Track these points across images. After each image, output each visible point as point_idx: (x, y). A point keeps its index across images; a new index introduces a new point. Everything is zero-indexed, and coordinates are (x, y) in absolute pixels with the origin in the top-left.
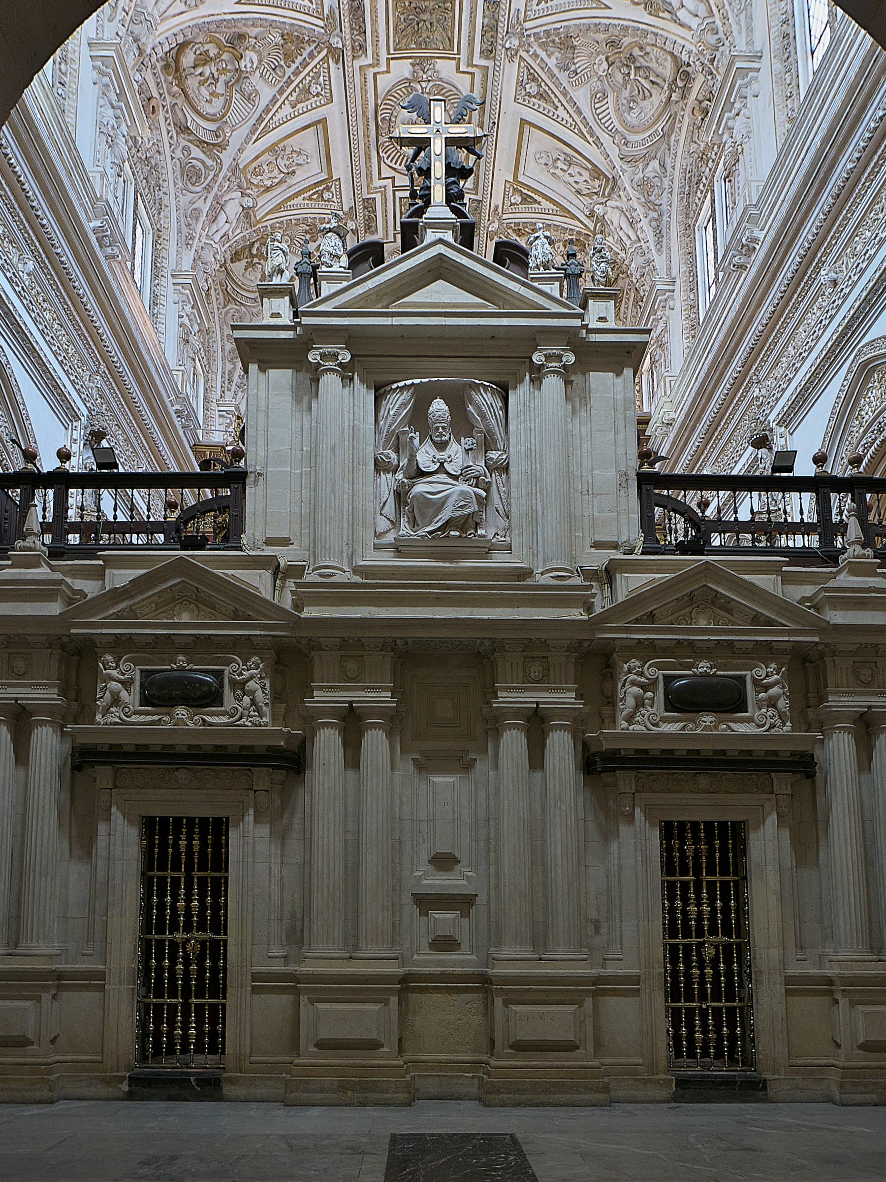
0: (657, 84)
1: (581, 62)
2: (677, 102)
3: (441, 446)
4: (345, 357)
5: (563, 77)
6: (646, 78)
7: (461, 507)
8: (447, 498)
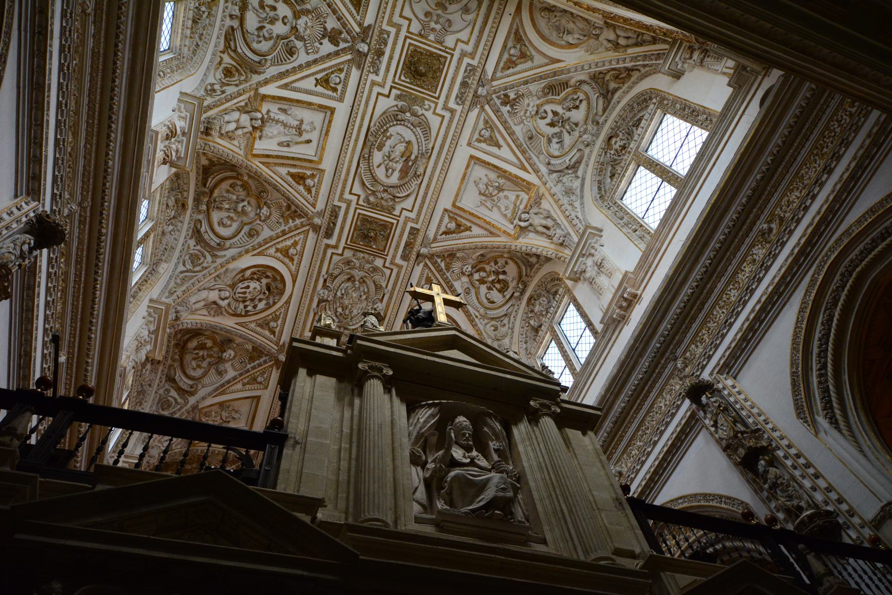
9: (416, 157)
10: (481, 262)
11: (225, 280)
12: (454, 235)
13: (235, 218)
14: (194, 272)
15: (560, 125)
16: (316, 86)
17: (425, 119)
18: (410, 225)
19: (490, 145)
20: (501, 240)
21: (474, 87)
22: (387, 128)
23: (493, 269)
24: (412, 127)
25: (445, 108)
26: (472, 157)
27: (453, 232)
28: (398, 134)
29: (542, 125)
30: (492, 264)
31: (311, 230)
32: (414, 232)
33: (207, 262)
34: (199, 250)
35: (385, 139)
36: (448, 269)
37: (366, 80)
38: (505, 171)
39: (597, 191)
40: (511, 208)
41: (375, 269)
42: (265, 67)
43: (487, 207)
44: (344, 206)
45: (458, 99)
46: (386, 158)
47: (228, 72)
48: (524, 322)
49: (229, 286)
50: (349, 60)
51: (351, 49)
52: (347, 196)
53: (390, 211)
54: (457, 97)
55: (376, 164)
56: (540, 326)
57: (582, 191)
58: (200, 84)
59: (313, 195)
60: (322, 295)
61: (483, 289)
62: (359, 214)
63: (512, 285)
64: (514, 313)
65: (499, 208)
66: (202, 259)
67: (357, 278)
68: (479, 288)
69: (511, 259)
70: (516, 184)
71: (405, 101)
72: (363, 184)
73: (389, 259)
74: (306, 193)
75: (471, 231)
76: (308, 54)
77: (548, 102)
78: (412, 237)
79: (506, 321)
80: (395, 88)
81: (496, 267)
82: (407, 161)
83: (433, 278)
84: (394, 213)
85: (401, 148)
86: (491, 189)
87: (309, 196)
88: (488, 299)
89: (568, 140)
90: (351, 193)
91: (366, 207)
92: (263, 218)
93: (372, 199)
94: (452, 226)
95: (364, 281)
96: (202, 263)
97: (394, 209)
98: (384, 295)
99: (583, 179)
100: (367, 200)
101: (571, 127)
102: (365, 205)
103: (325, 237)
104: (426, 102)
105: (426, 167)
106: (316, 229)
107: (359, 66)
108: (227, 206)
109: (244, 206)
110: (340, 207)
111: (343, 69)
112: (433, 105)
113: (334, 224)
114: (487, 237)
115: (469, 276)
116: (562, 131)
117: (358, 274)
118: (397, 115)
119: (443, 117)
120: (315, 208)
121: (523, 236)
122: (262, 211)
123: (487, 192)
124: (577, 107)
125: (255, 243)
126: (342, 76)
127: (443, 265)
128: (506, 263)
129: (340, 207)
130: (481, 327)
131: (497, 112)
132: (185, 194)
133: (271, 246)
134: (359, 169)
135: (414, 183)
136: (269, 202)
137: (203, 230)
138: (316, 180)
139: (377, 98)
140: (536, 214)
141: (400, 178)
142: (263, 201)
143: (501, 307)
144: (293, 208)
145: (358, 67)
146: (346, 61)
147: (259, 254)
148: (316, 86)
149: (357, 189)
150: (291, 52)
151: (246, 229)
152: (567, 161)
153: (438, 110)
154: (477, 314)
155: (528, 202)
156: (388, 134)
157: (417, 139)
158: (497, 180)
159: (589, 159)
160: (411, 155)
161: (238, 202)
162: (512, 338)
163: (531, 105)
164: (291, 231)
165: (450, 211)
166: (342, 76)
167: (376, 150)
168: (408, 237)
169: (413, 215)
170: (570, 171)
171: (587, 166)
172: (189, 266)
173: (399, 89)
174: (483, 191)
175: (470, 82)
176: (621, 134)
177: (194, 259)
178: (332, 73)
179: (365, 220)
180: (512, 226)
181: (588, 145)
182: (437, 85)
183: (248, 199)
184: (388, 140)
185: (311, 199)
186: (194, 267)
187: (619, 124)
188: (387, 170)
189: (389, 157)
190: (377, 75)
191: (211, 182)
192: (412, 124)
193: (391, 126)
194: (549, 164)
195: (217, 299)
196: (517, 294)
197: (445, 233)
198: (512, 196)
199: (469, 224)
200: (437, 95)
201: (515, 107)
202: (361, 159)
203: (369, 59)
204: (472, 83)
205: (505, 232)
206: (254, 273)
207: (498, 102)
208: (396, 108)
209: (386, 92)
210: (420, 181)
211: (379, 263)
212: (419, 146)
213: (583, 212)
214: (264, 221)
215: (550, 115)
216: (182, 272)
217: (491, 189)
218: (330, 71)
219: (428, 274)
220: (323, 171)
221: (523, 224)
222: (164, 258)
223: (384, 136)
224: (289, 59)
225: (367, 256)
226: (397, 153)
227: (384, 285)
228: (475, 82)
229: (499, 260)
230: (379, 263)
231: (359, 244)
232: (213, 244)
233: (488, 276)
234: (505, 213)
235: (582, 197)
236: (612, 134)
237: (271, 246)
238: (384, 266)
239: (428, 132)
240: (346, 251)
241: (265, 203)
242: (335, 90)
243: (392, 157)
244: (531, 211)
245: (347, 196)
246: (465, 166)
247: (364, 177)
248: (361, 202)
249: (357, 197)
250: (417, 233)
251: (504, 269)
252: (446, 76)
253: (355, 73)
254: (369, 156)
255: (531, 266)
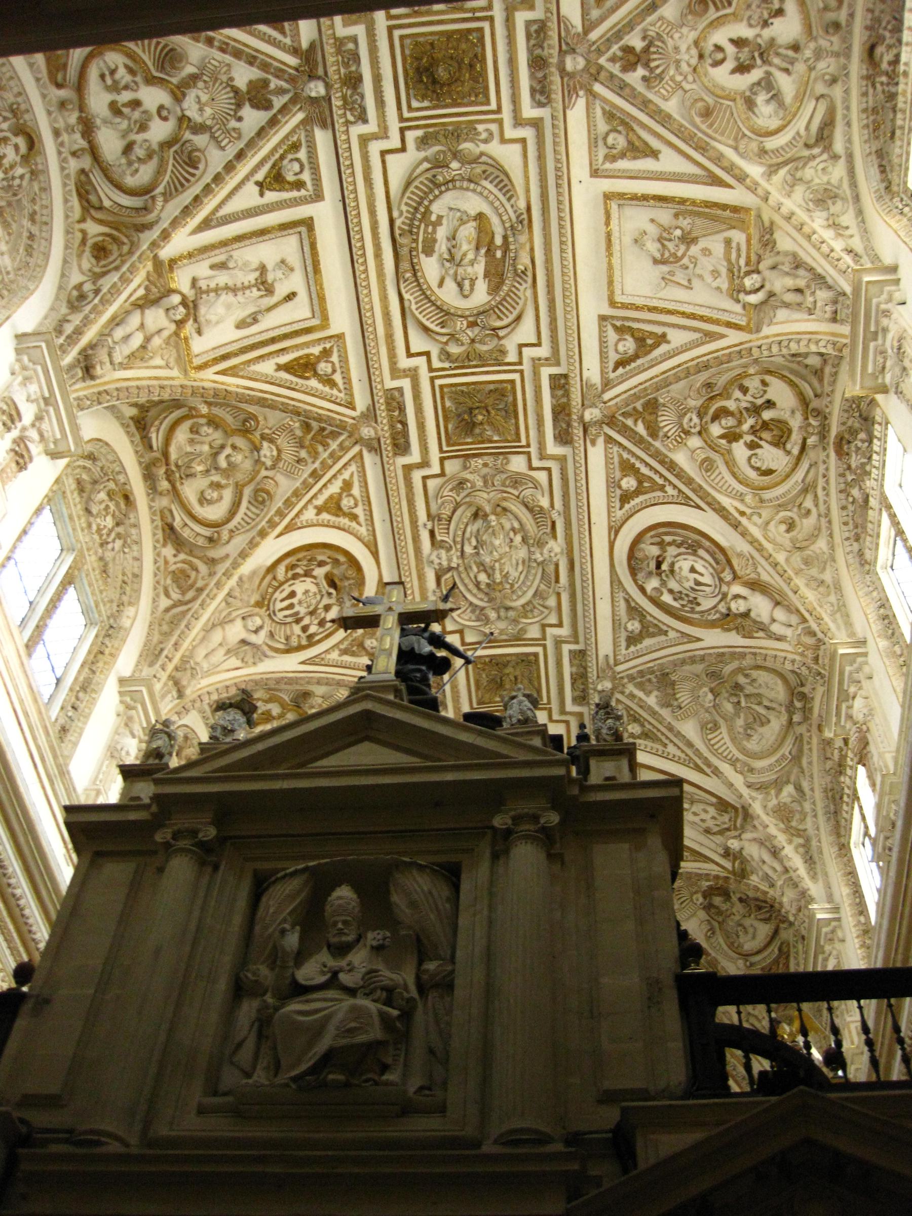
0: (773, 709)
1: (684, 697)
2: (799, 724)
3: (341, 950)
4: (211, 832)
5: (665, 713)
6: (759, 704)
7: (350, 1031)
8: (328, 1018)
9: (505, 238)
10: (711, 398)
11: (245, 597)
12: (639, 362)
13: (224, 482)
14: (187, 603)
15: (759, 62)
16: (262, 195)
17: (490, 161)
18: (546, 372)
19: (635, 158)
20: (734, 337)
21: (554, 60)
22: (427, 208)
23: (744, 405)
24: (472, 186)
25: (518, 122)
26: (608, 197)
27: (636, 357)
28: (451, 209)
29: (722, 76)
30: (737, 394)
31: (365, 453)
32: (560, 383)
33: (203, 578)
34: (184, 562)
35: (430, 229)
36: (654, 433)
37: (348, 141)
38: (683, 201)
39: (878, 176)
40: (724, 271)
41: (517, 480)
42: (156, 213)
43: (679, 284)
44: (405, 384)
45: (538, 96)
46: (447, 265)
47: (100, 251)
48: (843, 496)
49: (259, 604)
50: (303, 122)
51: (294, 100)
52: (404, 362)
53: (497, 357)
54: (533, 91)
55: (433, 281)
56: (866, 500)
57: (854, 184)
58: (57, 298)
59: (341, 386)
60: (437, 561)
61: (740, 451)
62: (441, 387)
63: (796, 422)
64: (821, 482)
65: (701, 277)
66: (193, 574)
67: (488, 509)
68: (729, 452)
69: (769, 372)
70: (714, 219)
71: (439, 142)
72: (426, 329)
73: (533, 450)
74: (327, 389)
75: (668, 342)
76: (223, 149)
77: (715, 24)
78: (560, 393)
79: (808, 503)
80: (409, 128)
81: (749, 397)
82: (490, 253)
83: (633, 460)
84: (508, 360)
85: (468, 231)
86: (670, 245)
87: (335, 392)
88: (757, 469)
89: (786, 84)
90: (410, 355)
91: (451, 368)
92: (269, 463)
93: (454, 349)
94: (629, 345)
95: (505, 509)
96: (195, 582)
97: (503, 352)
98: (554, 523)
99: (850, 157)
100: (446, 355)
101: (784, 58)
102: (447, 365)
103: (395, 454)
104: (480, 128)
105: (532, 249)
106: (374, 446)
107: (327, 123)
108: (200, 468)
109: (228, 456)
110: (400, 390)
111: (299, 140)
112: (494, 127)
113: (404, 424)
114: (703, 344)
115: (700, 433)
116: (768, 74)
117: (484, 499)
118: (434, 176)
119: (523, 141)
120: (354, 409)
121: (766, 321)
122: (262, 453)
123: (667, 255)
124: (780, 12)
125: (272, 512)
126: (302, 154)
127: (641, 429)
128: (764, 383)
129: (400, 390)
130: (756, 532)
131: (621, 88)
132: (121, 478)
133: (305, 507)
134: (406, 304)
135: (522, 288)
136: (267, 431)
137: (177, 524)
138: (335, 358)
139: (384, 162)
140: (774, 268)
141: (494, 289)
142: (257, 434)
143: (788, 476)
144: (315, 425)
145: (324, 126)
146: (297, 126)
147: (289, 529)
148: (262, 195)
149: (418, 343)
150: (191, 161)
151: (247, 492)
152: (803, 132)
153: (510, 133)
154: (742, 508)
155: (749, 249)
156: (433, 218)
157: (492, 203)
158: (675, 223)
159: (848, 108)
160: (493, 237)
161: (215, 455)
162: (831, 535)
163: (683, 48)
164: (326, 467)
165: (613, 317)
166: (302, 154)
167: (422, 256)
168: (553, 396)
169: (543, 351)
170: (816, 151)
171: (848, 124)
172: (176, 595)
173: (417, 127)
174: (658, 256)
175: (545, 53)
176: (887, 34)
177: (181, 578)
178: (282, 158)
179: (460, 394)
180: (738, 308)
181: (834, 81)
182: (486, 88)
183: (230, 442)
184: (439, 228)
185: (342, 395)
186: (183, 594)
187: (877, 14)
188: (460, 285)
189: (452, 259)
190: (365, 121)
191: (157, 439)
192: (470, 181)
193: (431, 202)
194: (763, 152)
195: (244, 635)
196: (811, 441)
197: (620, 364)
198: (716, 244)
199: (658, 330)
200: (493, 106)
201: (653, 64)
202: (402, 286)
203: (337, 102)
204: (551, 56)
205: (729, 325)
206: (293, 567)
207: (615, 69)
208: (426, 165)
209: (395, 143)
210: (530, 280)
211: (518, 464)
212: (500, 216)
213: (865, 232)
214: (273, 467)
215: (730, 49)
216: (167, 610)
217: (670, 245)
218: (277, 156)
219: (620, 456)
220: (340, 337)
221: (753, 299)
222: (125, 599)
223: (427, 226)
224: (193, 175)
225: (489, 460)
226: (466, 247)
227: (545, 502)
228: (555, 52)
229: (747, 383)
230: (518, 464)
231: (467, 444)
232: (201, 542)
233: (740, 423)
234: (715, 284)
235: (857, 198)
236: (873, 40)
237: (305, 507)
238: (531, 468)
239: (506, 181)
240: (447, 463)
241: (263, 437)
242: (299, 185)
243: (458, 258)
244: (761, 267)
245: (404, 362)
246: (603, 219)
247: (420, 317)
248: (436, 364)
249: (424, 358)
250: (567, 383)
251: (767, 397)
252: (495, 62)
253: (321, 137)
254: (415, 275)
255: (818, 373)
